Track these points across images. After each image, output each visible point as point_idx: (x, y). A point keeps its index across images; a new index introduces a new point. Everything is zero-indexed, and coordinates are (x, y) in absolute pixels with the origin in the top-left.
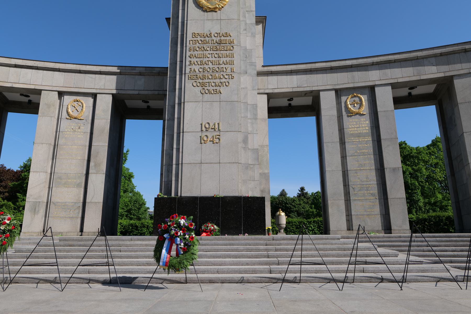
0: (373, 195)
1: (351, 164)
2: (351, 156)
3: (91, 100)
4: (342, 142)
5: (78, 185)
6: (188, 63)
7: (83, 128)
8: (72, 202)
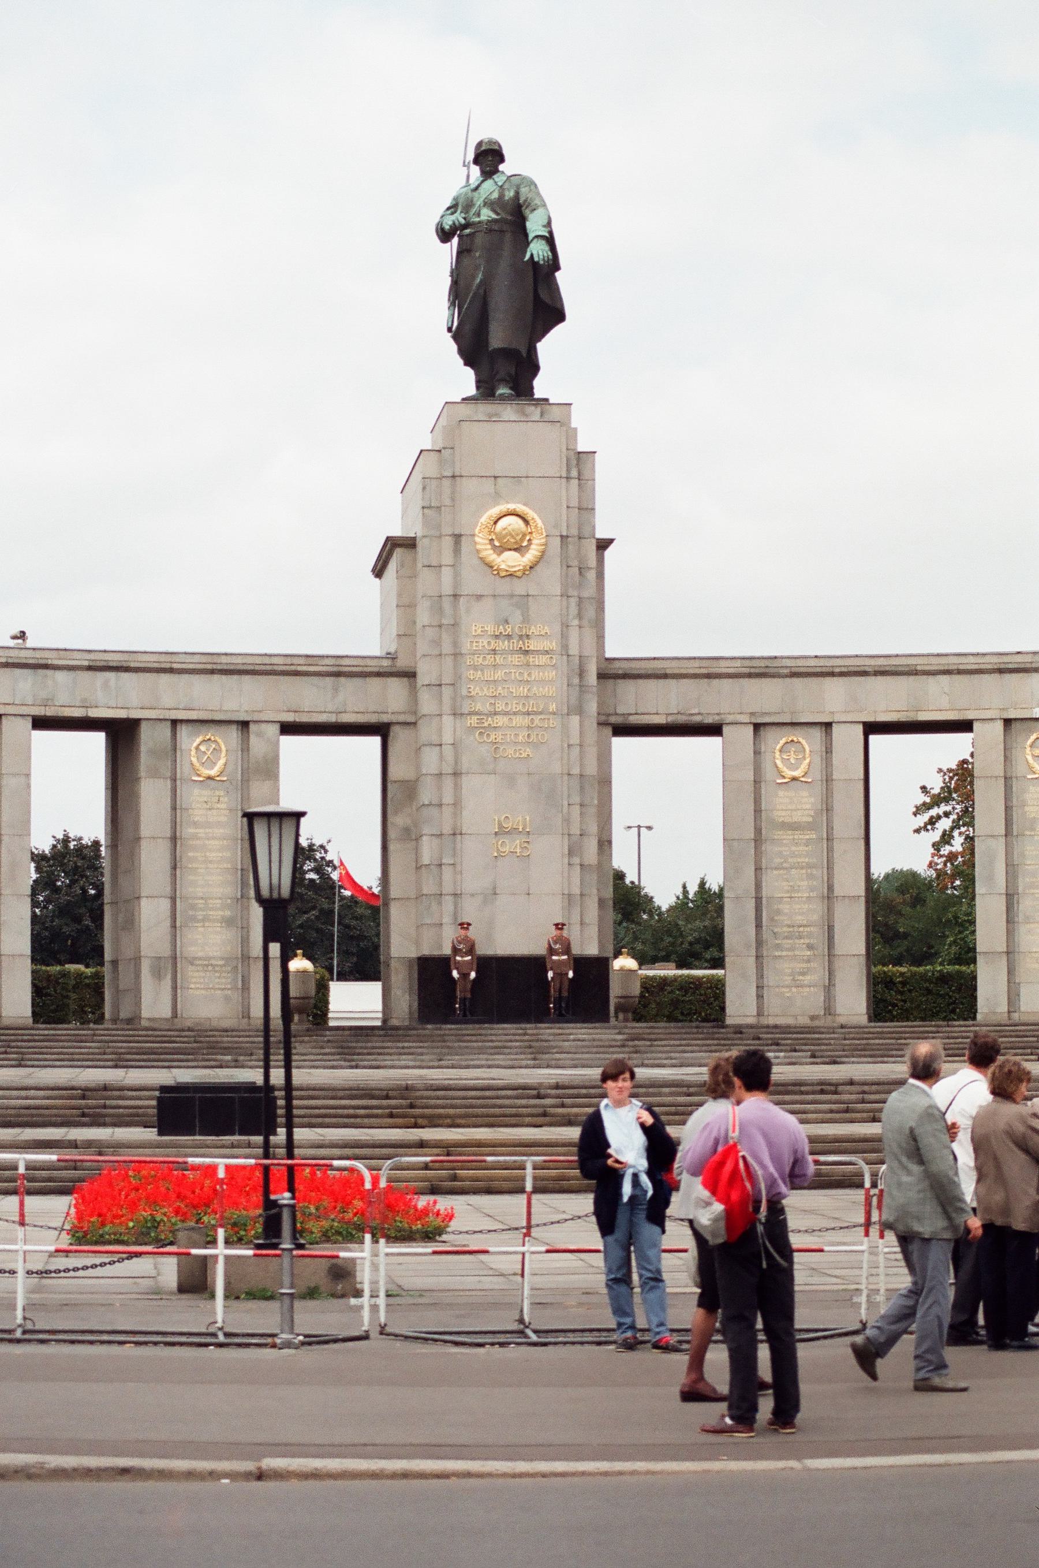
0: (810, 947)
1: (774, 885)
2: (776, 869)
3: (234, 732)
4: (758, 840)
5: (229, 922)
6: (464, 692)
7: (226, 799)
8: (222, 959)
